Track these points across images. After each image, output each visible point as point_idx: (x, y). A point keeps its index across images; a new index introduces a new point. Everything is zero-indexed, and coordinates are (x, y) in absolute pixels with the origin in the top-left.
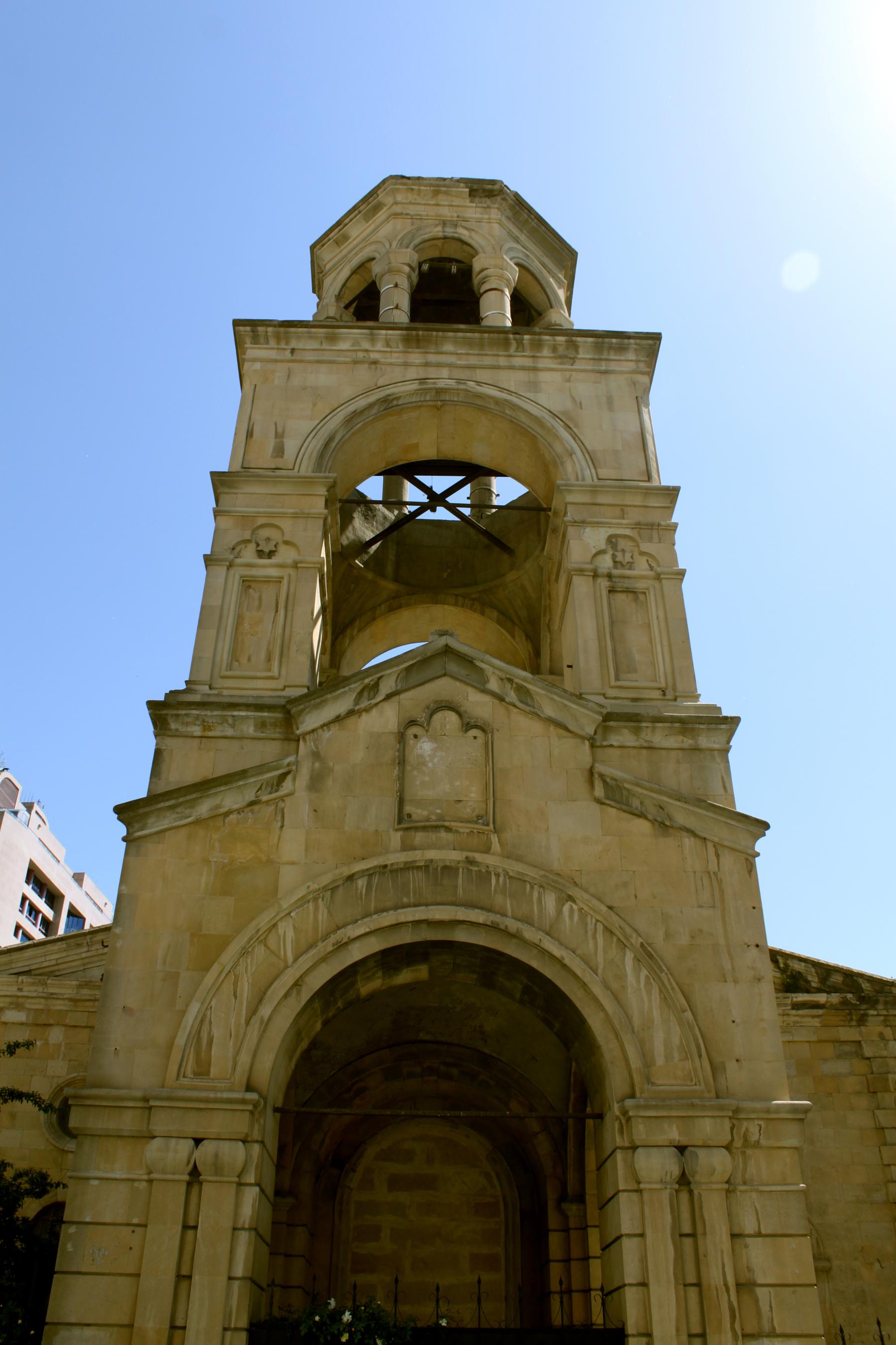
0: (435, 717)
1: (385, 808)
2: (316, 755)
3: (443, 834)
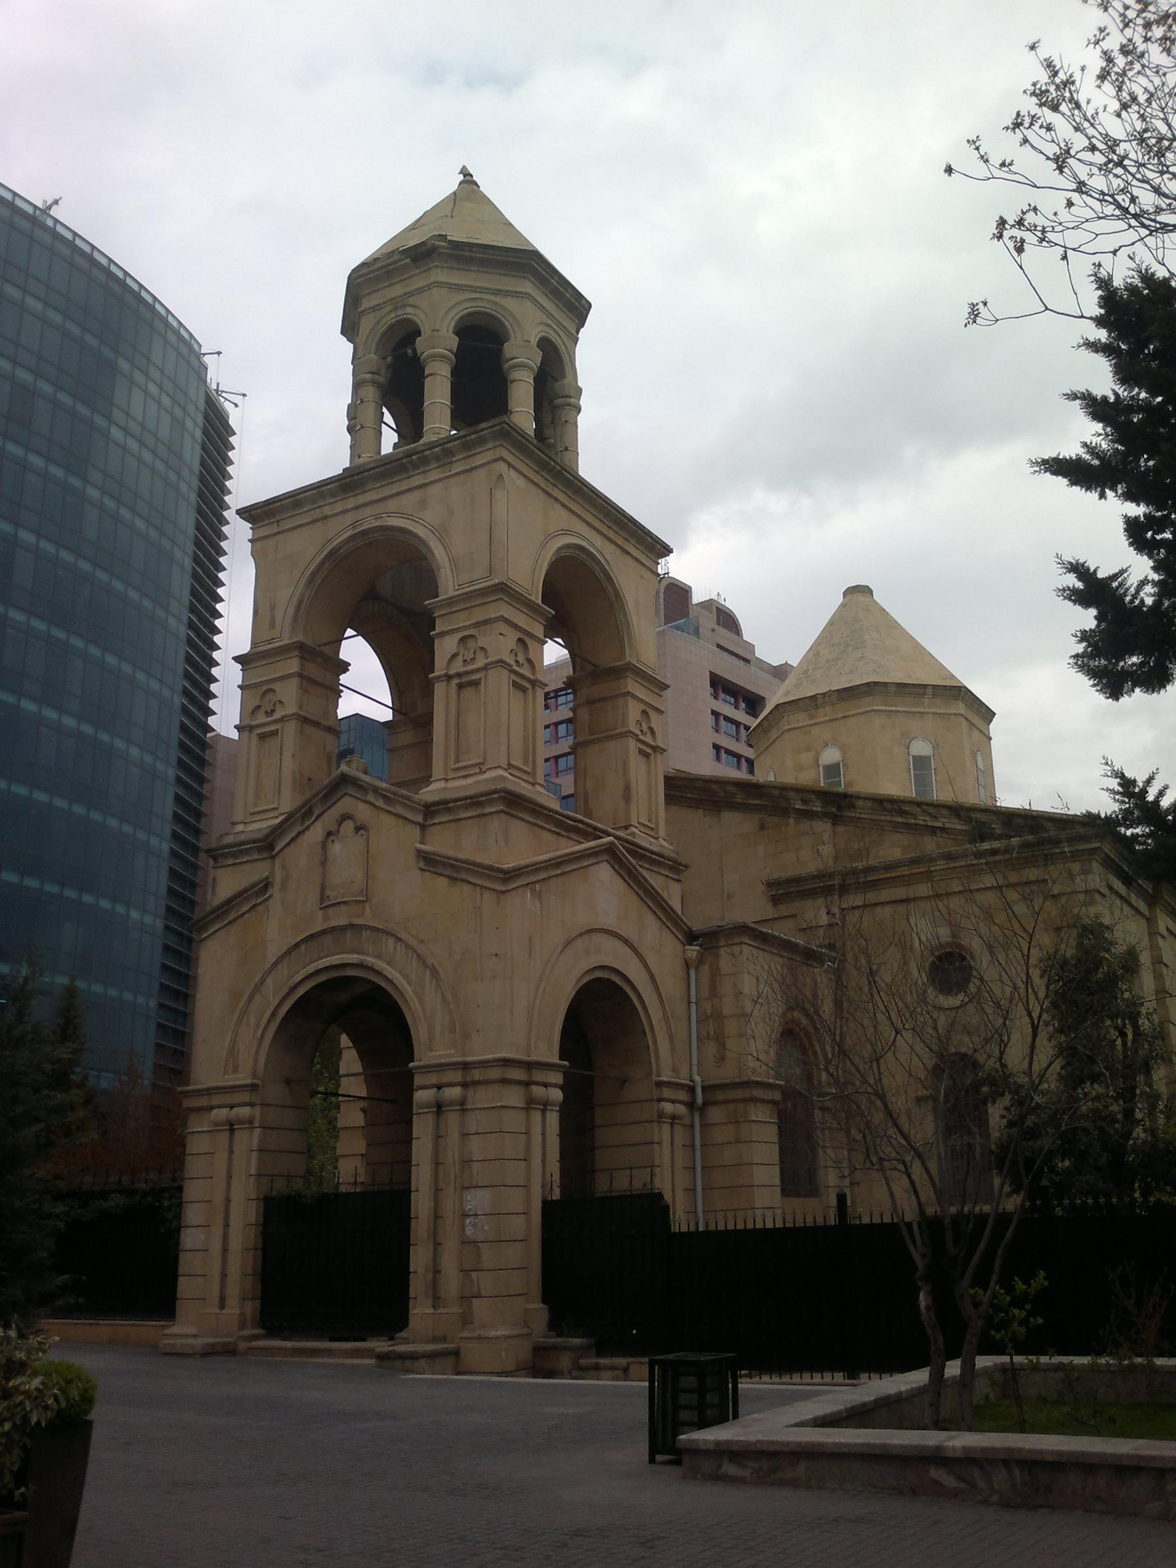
0: (345, 824)
1: (315, 895)
2: (284, 867)
3: (343, 907)
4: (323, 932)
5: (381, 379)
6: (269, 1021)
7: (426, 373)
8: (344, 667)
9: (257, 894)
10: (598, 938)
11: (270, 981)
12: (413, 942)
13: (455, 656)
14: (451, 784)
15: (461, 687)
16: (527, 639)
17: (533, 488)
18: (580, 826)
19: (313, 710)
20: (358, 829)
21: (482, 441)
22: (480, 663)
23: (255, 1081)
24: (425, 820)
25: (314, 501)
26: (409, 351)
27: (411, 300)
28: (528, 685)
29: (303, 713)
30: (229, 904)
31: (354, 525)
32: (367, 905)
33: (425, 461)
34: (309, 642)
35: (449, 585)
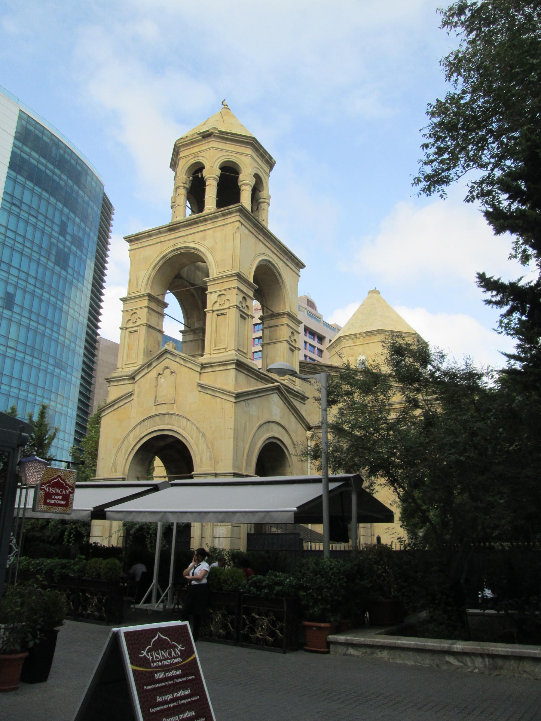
2: (139, 387)
3: (164, 405)
4: (156, 415)
5: (187, 186)
6: (131, 452)
7: (207, 184)
8: (166, 305)
9: (127, 398)
10: (273, 424)
11: (131, 435)
12: (195, 422)
13: (216, 302)
14: (212, 356)
15: (218, 315)
16: (246, 297)
17: (251, 234)
18: (266, 377)
19: (153, 323)
20: (172, 373)
21: (230, 213)
22: (226, 306)
23: (124, 476)
24: (201, 369)
25: (157, 234)
26: (200, 176)
27: (201, 154)
28: (246, 317)
29: (149, 323)
30: (115, 402)
31: (174, 245)
32: (175, 405)
33: (206, 220)
34: (153, 294)
35: (214, 273)
